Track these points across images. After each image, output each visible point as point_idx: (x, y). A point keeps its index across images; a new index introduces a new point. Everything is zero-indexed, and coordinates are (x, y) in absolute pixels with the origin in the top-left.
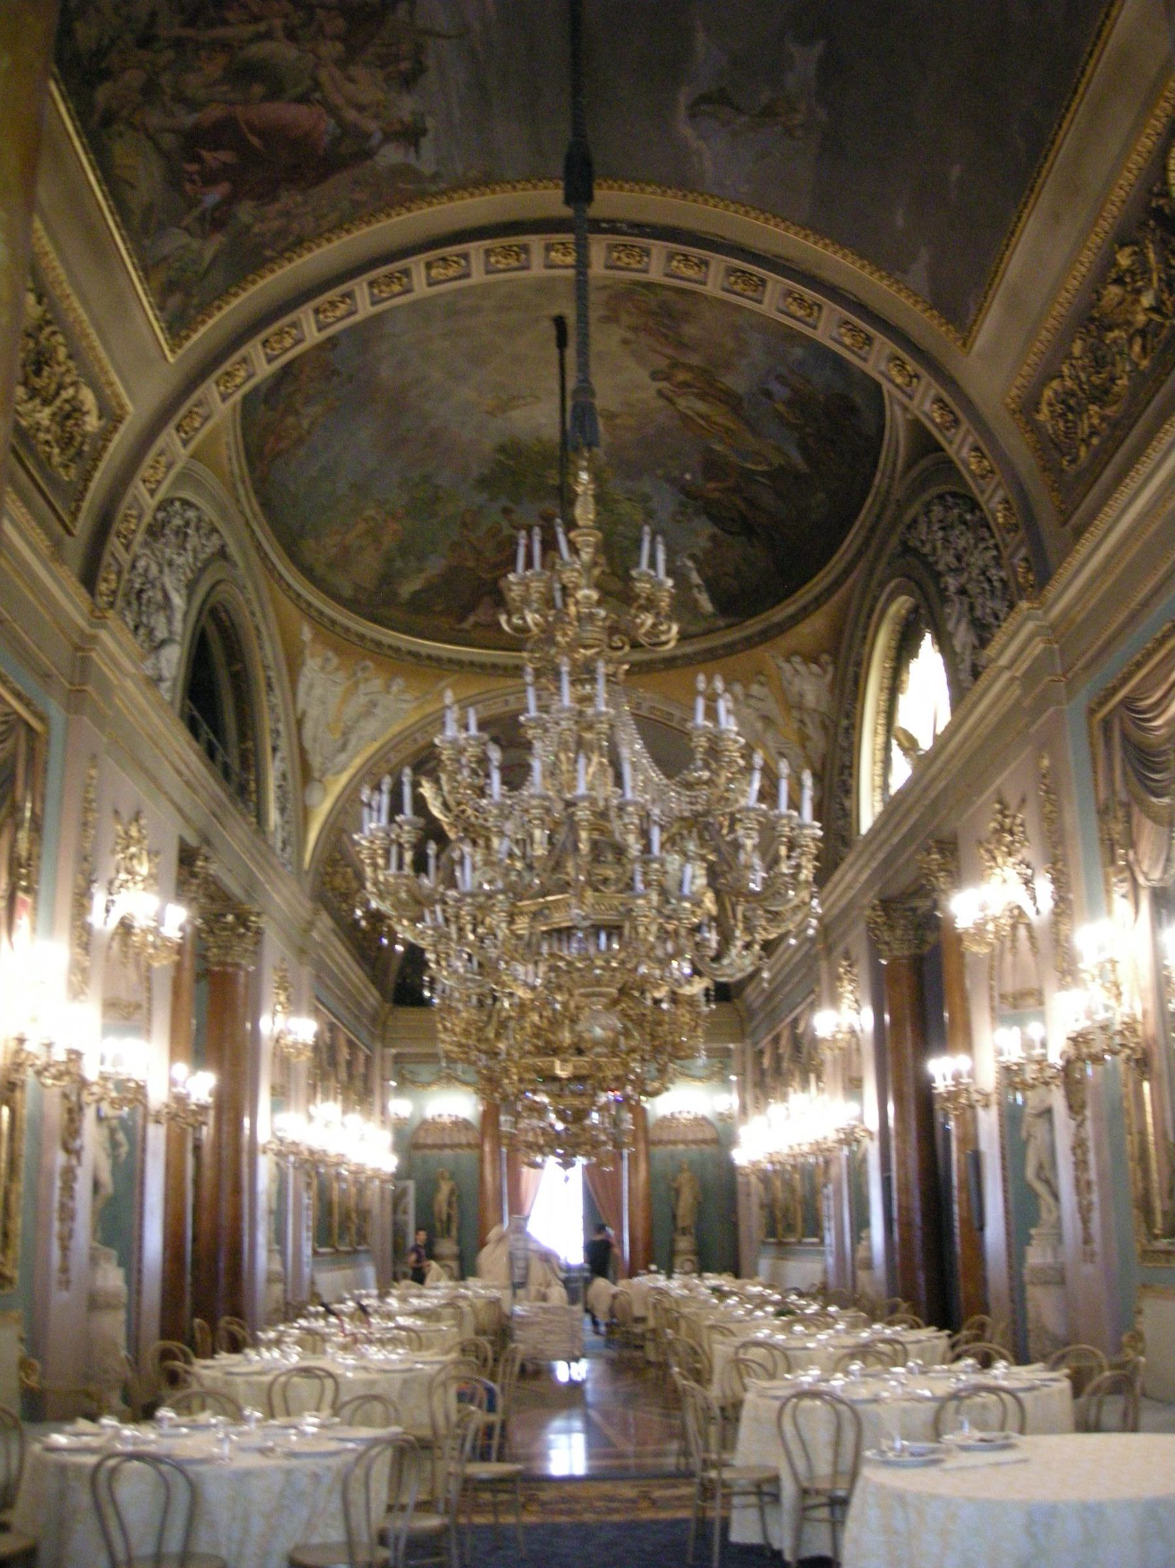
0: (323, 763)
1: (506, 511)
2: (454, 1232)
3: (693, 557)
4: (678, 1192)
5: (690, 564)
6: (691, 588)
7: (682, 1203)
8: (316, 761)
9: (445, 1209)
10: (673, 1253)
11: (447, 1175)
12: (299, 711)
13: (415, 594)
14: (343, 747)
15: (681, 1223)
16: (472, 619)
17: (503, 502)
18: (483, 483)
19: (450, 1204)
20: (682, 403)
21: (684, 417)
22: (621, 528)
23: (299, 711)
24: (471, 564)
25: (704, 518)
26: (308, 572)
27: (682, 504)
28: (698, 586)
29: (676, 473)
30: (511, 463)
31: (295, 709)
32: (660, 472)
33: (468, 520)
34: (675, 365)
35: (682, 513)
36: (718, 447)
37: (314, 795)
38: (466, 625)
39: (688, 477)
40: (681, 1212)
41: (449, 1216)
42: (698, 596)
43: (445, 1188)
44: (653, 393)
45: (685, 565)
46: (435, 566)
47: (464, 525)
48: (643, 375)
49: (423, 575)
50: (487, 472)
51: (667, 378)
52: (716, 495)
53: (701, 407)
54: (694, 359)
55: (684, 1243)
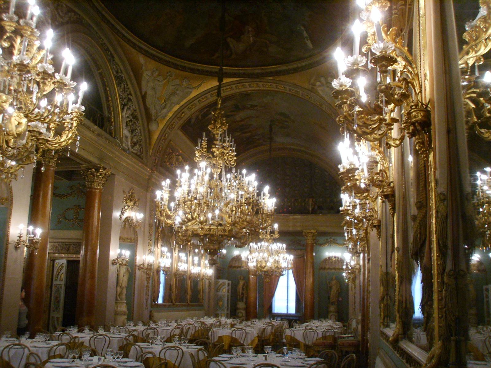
0: (157, 113)
2: (244, 300)
4: (331, 287)
5: (303, 28)
7: (332, 293)
8: (153, 112)
9: (241, 291)
10: (328, 312)
11: (242, 278)
12: (143, 93)
14: (164, 108)
15: (332, 300)
16: (217, 55)
19: (243, 289)
23: (143, 93)
26: (141, 36)
28: (306, 37)
31: (141, 92)
37: (153, 127)
38: (214, 58)
40: (331, 297)
41: (242, 294)
43: (241, 283)
55: (332, 308)
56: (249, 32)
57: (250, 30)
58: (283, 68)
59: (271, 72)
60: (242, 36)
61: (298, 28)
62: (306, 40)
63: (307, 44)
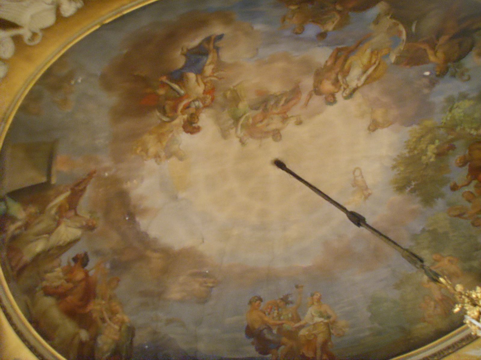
1: (454, 188)
17: (446, 189)
18: (428, 200)
20: (353, 85)
21: (369, 80)
25: (464, 61)
27: (453, 76)
29: (425, 81)
30: (413, 183)
32: (426, 91)
33: (457, 213)
34: (317, 91)
35: (462, 74)
39: (427, 73)
44: (348, 102)
47: (460, 216)
48: (331, 110)
50: (419, 199)
51: (333, 95)
52: (440, 54)
54: (308, 82)
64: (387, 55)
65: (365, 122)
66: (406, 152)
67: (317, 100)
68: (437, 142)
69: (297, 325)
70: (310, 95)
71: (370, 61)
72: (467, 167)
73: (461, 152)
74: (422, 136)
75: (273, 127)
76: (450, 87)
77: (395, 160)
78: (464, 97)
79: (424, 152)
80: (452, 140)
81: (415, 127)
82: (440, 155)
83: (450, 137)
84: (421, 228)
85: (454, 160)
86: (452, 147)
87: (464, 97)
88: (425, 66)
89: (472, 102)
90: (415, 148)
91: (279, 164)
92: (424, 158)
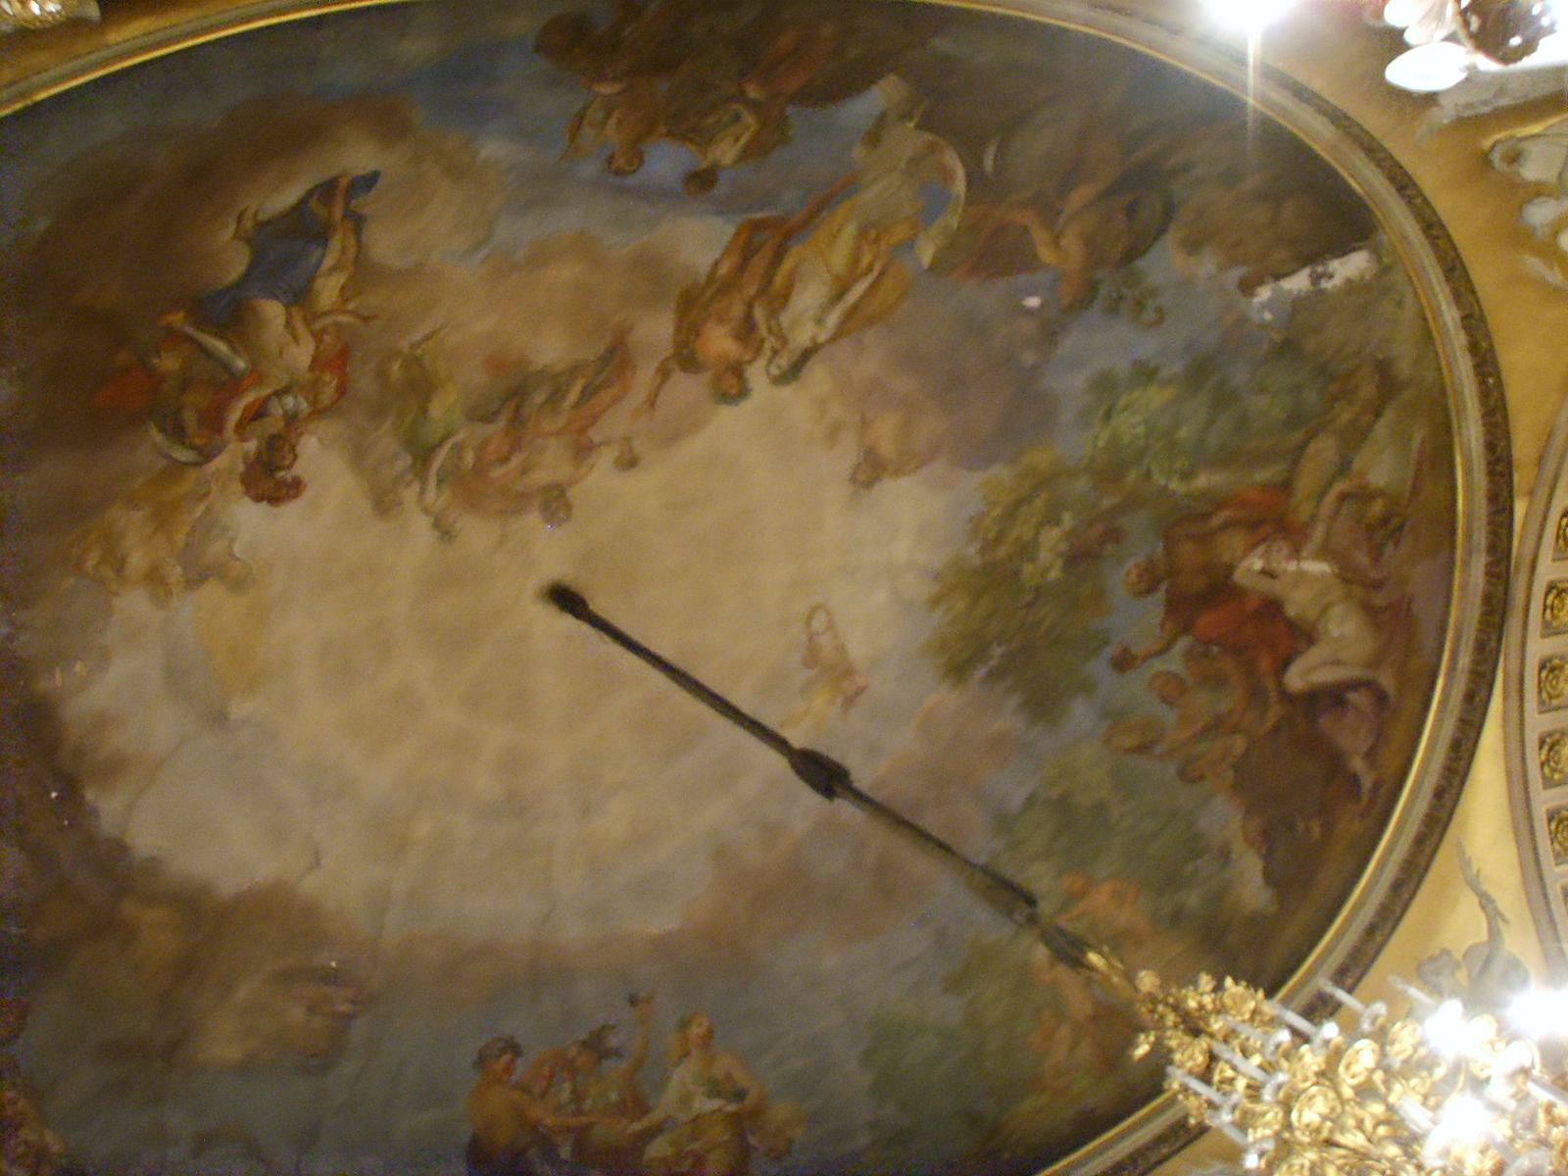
1: (1124, 662)
3: (1248, 287)
5: (1264, 293)
6: (1322, 292)
13: (1269, 877)
16: (1358, 764)
17: (1098, 668)
18: (1043, 705)
20: (802, 337)
22: (1183, 433)
24: (1239, 743)
25: (1141, 264)
27: (1113, 309)
28: (1316, 279)
29: (1028, 327)
30: (997, 651)
32: (1029, 358)
33: (1129, 741)
34: (686, 357)
35: (1140, 305)
36: (926, 253)
38: (1367, 782)
39: (1033, 302)
42: (1337, 281)
44: (786, 392)
45: (1267, 305)
46: (1224, 818)
47: (1142, 749)
48: (727, 417)
49: (1238, 847)
50: (1013, 701)
51: (737, 370)
52: (1072, 243)
53: (808, 297)
54: (657, 330)
56: (1268, 573)
57: (1258, 564)
58: (1471, 434)
59: (1493, 498)
60: (1291, 611)
61: (1268, 316)
62: (1326, 285)
63: (1349, 281)
64: (909, 244)
65: (846, 455)
66: (972, 550)
67: (686, 389)
68: (1068, 520)
69: (637, 1126)
70: (664, 373)
71: (855, 260)
72: (1160, 596)
73: (1141, 546)
74: (1020, 502)
75: (541, 477)
76: (1102, 345)
77: (937, 577)
78: (1146, 374)
79: (1027, 550)
80: (1115, 512)
81: (1001, 472)
82: (1080, 558)
83: (1107, 503)
84: (1023, 792)
85: (1120, 575)
86: (1114, 535)
87: (1146, 374)
88: (1022, 279)
89: (1168, 394)
90: (1000, 538)
91: (566, 599)
92: (1028, 569)
